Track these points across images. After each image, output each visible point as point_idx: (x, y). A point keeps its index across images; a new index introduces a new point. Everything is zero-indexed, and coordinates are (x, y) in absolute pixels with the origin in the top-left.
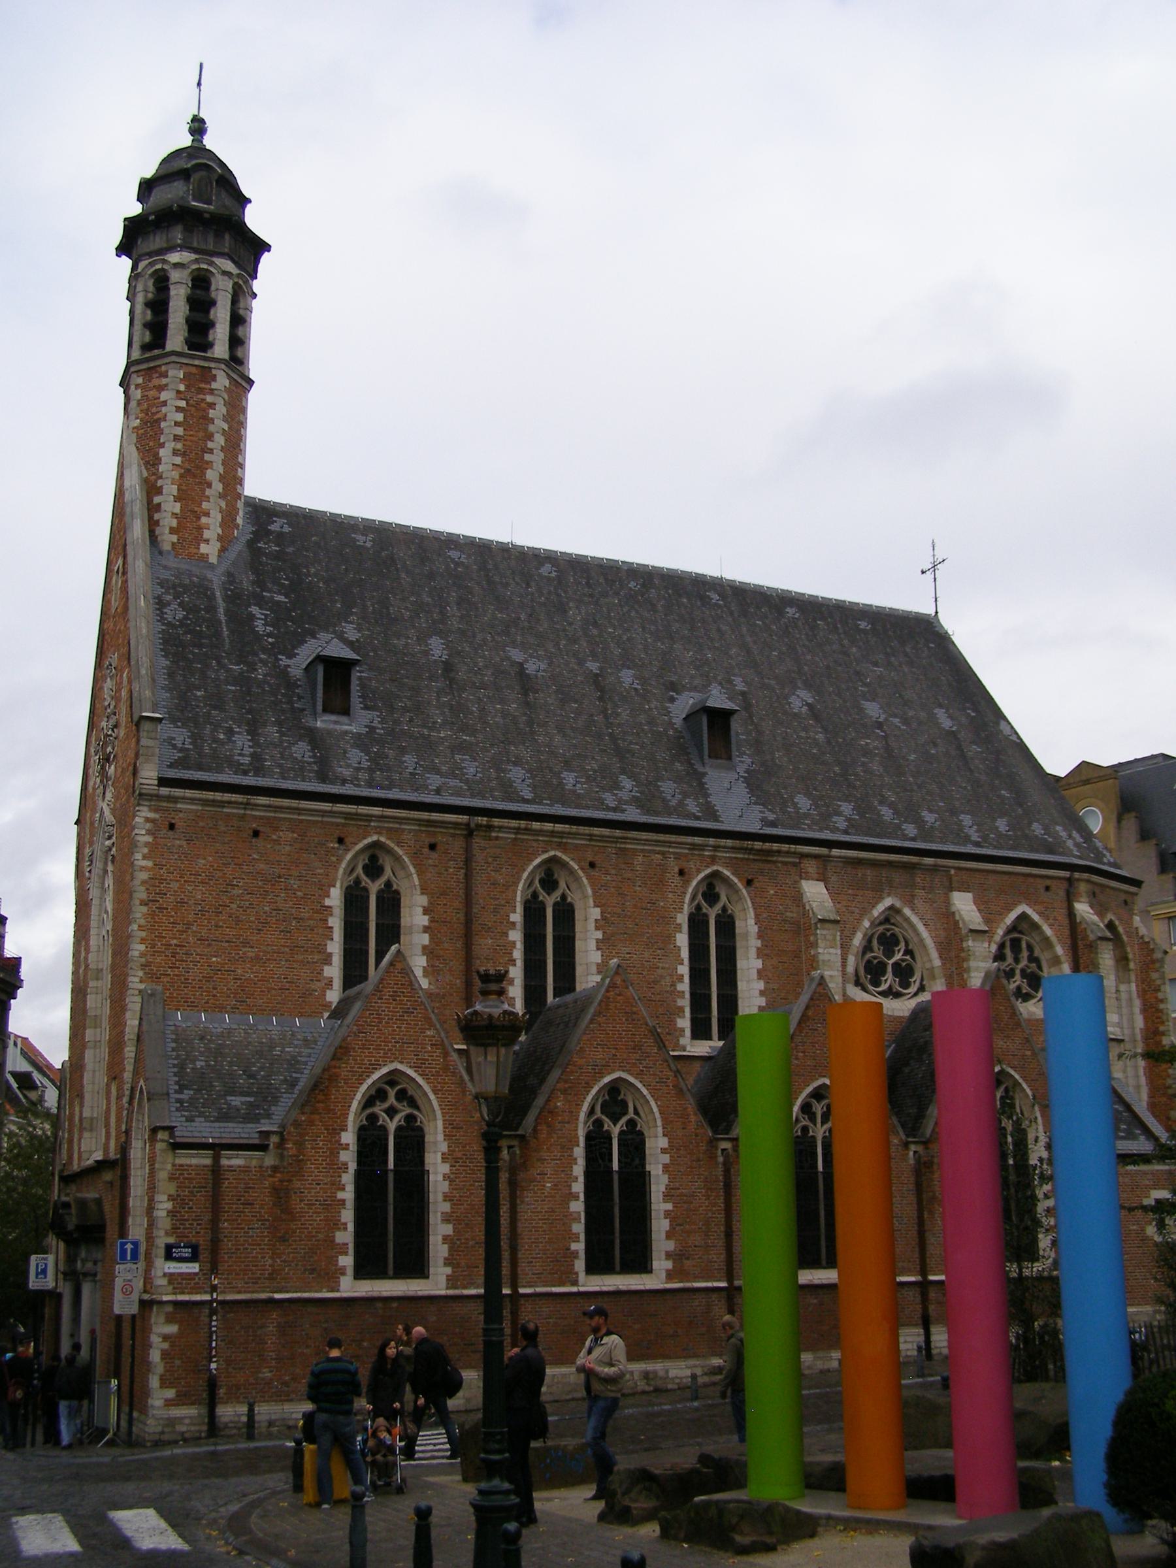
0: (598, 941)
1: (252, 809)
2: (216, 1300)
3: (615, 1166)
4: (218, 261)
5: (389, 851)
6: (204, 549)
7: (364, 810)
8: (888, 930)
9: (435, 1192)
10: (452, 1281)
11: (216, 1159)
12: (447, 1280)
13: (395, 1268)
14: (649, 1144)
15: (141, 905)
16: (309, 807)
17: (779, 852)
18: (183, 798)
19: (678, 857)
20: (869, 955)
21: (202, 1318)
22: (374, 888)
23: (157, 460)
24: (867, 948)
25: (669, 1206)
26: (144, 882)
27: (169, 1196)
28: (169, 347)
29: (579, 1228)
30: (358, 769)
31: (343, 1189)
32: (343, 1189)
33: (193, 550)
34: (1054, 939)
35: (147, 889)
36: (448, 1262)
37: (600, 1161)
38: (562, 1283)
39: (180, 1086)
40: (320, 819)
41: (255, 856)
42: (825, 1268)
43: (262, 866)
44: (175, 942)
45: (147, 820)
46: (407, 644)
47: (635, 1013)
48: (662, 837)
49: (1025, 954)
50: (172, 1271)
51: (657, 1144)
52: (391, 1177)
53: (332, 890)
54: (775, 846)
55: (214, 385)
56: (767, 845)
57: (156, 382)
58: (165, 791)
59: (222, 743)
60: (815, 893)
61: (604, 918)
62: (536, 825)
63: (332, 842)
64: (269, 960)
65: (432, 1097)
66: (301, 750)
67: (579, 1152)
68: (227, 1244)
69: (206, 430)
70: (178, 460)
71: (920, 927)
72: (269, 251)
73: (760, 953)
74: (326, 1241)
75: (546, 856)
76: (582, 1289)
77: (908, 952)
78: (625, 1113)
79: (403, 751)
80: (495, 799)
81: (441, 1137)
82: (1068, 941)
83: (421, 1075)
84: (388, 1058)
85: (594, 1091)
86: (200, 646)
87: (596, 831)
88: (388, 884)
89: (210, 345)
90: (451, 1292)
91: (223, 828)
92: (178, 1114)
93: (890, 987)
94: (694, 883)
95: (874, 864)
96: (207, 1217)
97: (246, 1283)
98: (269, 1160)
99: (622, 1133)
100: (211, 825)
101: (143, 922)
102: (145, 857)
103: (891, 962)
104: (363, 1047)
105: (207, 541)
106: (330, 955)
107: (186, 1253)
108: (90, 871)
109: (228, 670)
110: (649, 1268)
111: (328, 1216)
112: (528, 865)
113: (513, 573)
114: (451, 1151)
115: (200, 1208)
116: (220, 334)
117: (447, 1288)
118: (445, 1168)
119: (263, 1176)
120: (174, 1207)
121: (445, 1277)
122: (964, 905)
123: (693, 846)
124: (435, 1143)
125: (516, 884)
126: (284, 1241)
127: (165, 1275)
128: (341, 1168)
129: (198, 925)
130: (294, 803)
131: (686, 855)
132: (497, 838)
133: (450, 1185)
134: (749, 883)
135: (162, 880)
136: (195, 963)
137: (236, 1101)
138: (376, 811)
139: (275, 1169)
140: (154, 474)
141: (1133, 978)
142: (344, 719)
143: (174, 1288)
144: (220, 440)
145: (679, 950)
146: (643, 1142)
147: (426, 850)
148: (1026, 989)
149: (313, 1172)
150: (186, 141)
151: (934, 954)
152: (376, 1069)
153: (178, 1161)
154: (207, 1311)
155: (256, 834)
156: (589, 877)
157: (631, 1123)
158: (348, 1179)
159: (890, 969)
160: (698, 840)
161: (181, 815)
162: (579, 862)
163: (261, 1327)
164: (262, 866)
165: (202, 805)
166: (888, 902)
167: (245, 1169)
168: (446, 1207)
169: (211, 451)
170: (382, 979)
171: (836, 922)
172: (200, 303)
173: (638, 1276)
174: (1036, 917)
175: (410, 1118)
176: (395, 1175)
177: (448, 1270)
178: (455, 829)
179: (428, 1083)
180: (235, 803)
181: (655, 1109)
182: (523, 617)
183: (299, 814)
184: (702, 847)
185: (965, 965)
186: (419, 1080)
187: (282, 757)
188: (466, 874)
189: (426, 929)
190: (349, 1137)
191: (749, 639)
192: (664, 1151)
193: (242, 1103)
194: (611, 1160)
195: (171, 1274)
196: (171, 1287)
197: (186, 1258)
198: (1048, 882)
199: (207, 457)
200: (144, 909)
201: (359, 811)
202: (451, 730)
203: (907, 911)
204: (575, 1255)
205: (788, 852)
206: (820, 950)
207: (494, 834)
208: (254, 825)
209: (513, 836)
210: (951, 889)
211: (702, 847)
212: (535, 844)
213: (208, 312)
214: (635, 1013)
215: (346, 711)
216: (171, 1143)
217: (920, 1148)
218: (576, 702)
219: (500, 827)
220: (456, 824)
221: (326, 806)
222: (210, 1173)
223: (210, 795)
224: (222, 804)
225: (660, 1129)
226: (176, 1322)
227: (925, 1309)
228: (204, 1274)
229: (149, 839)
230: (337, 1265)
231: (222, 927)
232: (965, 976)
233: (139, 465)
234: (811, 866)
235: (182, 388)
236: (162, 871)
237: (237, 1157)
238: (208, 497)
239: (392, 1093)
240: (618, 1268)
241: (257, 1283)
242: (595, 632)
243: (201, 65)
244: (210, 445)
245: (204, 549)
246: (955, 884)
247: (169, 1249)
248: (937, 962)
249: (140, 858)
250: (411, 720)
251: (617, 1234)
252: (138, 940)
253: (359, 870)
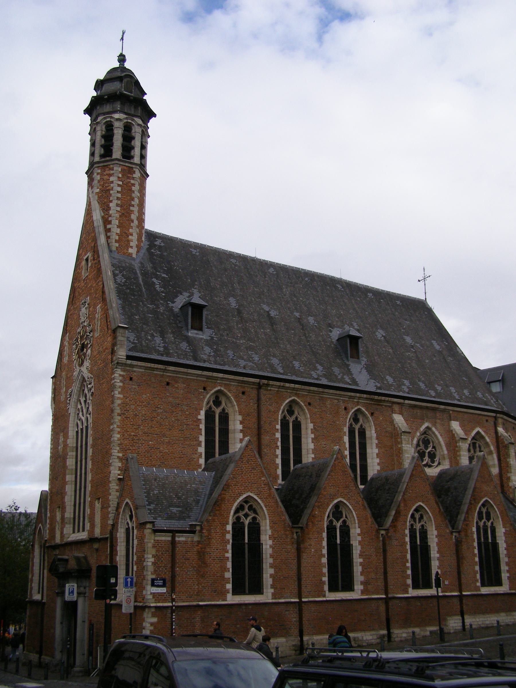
0: (312, 438)
1: (166, 372)
2: (174, 606)
3: (338, 541)
4: (136, 119)
5: (225, 394)
6: (130, 250)
7: (215, 374)
8: (426, 437)
9: (266, 554)
10: (274, 596)
11: (173, 537)
12: (272, 595)
13: (249, 590)
14: (352, 531)
15: (118, 415)
16: (191, 372)
17: (384, 401)
18: (137, 366)
19: (344, 401)
20: (419, 448)
21: (168, 615)
22: (218, 411)
23: (109, 208)
24: (418, 445)
25: (361, 560)
26: (119, 405)
27: (153, 555)
28: (114, 156)
29: (325, 570)
30: (210, 356)
31: (228, 552)
32: (228, 552)
33: (126, 251)
34: (490, 443)
35: (121, 408)
36: (272, 586)
37: (332, 539)
38: (319, 596)
39: (149, 502)
40: (195, 378)
41: (168, 394)
42: (422, 589)
43: (171, 399)
44: (133, 434)
45: (120, 375)
46: (220, 300)
47: (346, 471)
48: (338, 392)
49: (478, 449)
50: (154, 591)
51: (355, 531)
52: (246, 546)
53: (201, 411)
54: (383, 398)
55: (134, 176)
56: (380, 398)
57: (107, 172)
58: (129, 362)
59: (150, 341)
60: (399, 419)
61: (315, 428)
62: (287, 385)
63: (201, 389)
64: (174, 443)
65: (264, 509)
66: (184, 345)
67: (325, 535)
68: (178, 579)
69: (131, 196)
70: (119, 209)
72: (155, 117)
73: (377, 446)
74: (221, 577)
75: (290, 399)
76: (328, 599)
77: (434, 447)
78: (342, 517)
79: (226, 348)
80: (268, 372)
81: (268, 528)
82: (495, 444)
83: (260, 498)
84: (246, 491)
85: (330, 507)
86: (134, 295)
87: (312, 388)
88: (224, 410)
89: (132, 157)
90: (274, 601)
91: (154, 381)
92: (149, 516)
93: (427, 463)
94: (351, 413)
95: (421, 407)
96: (169, 565)
97: (187, 597)
98: (196, 538)
99: (341, 526)
100: (148, 379)
101: (118, 424)
102: (119, 393)
103: (427, 451)
104: (235, 485)
105: (132, 247)
106: (201, 442)
107: (161, 583)
108: (70, 400)
109: (148, 307)
110: (353, 589)
111: (221, 565)
112: (283, 403)
113: (258, 270)
114: (273, 534)
115: (166, 561)
116: (137, 152)
117: (272, 599)
118: (270, 542)
119: (194, 546)
120: (155, 561)
121: (271, 594)
122: (455, 426)
123: (350, 397)
124: (266, 530)
125: (278, 411)
126: (203, 577)
127: (151, 593)
128: (227, 542)
129: (143, 426)
130: (185, 370)
131: (347, 401)
132: (270, 390)
133: (273, 550)
134: (372, 414)
135: (127, 404)
136: (142, 444)
137: (174, 510)
138: (221, 375)
139: (199, 542)
140: (107, 214)
142: (200, 332)
143: (155, 600)
144: (137, 201)
145: (345, 444)
146: (349, 531)
147: (241, 394)
149: (215, 544)
150: (117, 65)
151: (444, 448)
152: (241, 495)
153: (157, 538)
154: (170, 611)
155: (168, 384)
156: (308, 409)
157: (344, 522)
158: (229, 547)
159: (427, 454)
160: (352, 394)
161: (135, 374)
162: (304, 402)
163: (193, 619)
164: (171, 399)
165: (145, 369)
166: (426, 425)
167: (185, 542)
168: (271, 560)
169: (133, 206)
170: (243, 453)
171: (409, 433)
172: (128, 138)
173: (348, 593)
174: (483, 433)
175: (254, 519)
176: (248, 545)
177: (272, 590)
178: (253, 385)
179: (263, 502)
180: (160, 369)
181: (355, 515)
182: (265, 291)
183: (187, 375)
184: (354, 397)
185: (458, 453)
186: (259, 500)
187: (177, 349)
188: (258, 406)
189: (241, 431)
190: (229, 528)
191: (356, 306)
192: (359, 535)
193: (177, 511)
194: (336, 539)
195: (154, 593)
196: (154, 599)
197: (160, 585)
198: (487, 418)
199: (131, 208)
200: (119, 418)
201: (214, 375)
202: (245, 339)
203: (434, 429)
204: (324, 583)
205: (388, 401)
206: (403, 445)
207: (269, 388)
208: (167, 380)
209: (277, 389)
210: (451, 420)
211: (354, 397)
212: (286, 393)
213: (130, 142)
214: (346, 471)
215: (201, 329)
216: (153, 530)
217: (457, 534)
218: (293, 330)
219: (272, 385)
220: (254, 383)
221: (199, 372)
222: (170, 544)
223: (149, 365)
224: (153, 369)
225: (357, 525)
226: (156, 617)
227: (462, 607)
228: (168, 593)
229: (121, 384)
230: (225, 588)
231: (154, 427)
232: (458, 458)
233: (100, 210)
234: (396, 408)
235: (120, 176)
236: (127, 400)
237: (182, 536)
238: (132, 227)
239: (246, 507)
240: (340, 589)
241: (191, 597)
242: (295, 299)
244: (133, 203)
245: (130, 250)
246: (452, 418)
247: (153, 580)
248: (446, 452)
249: (117, 393)
250: (228, 335)
251: (340, 573)
252: (117, 432)
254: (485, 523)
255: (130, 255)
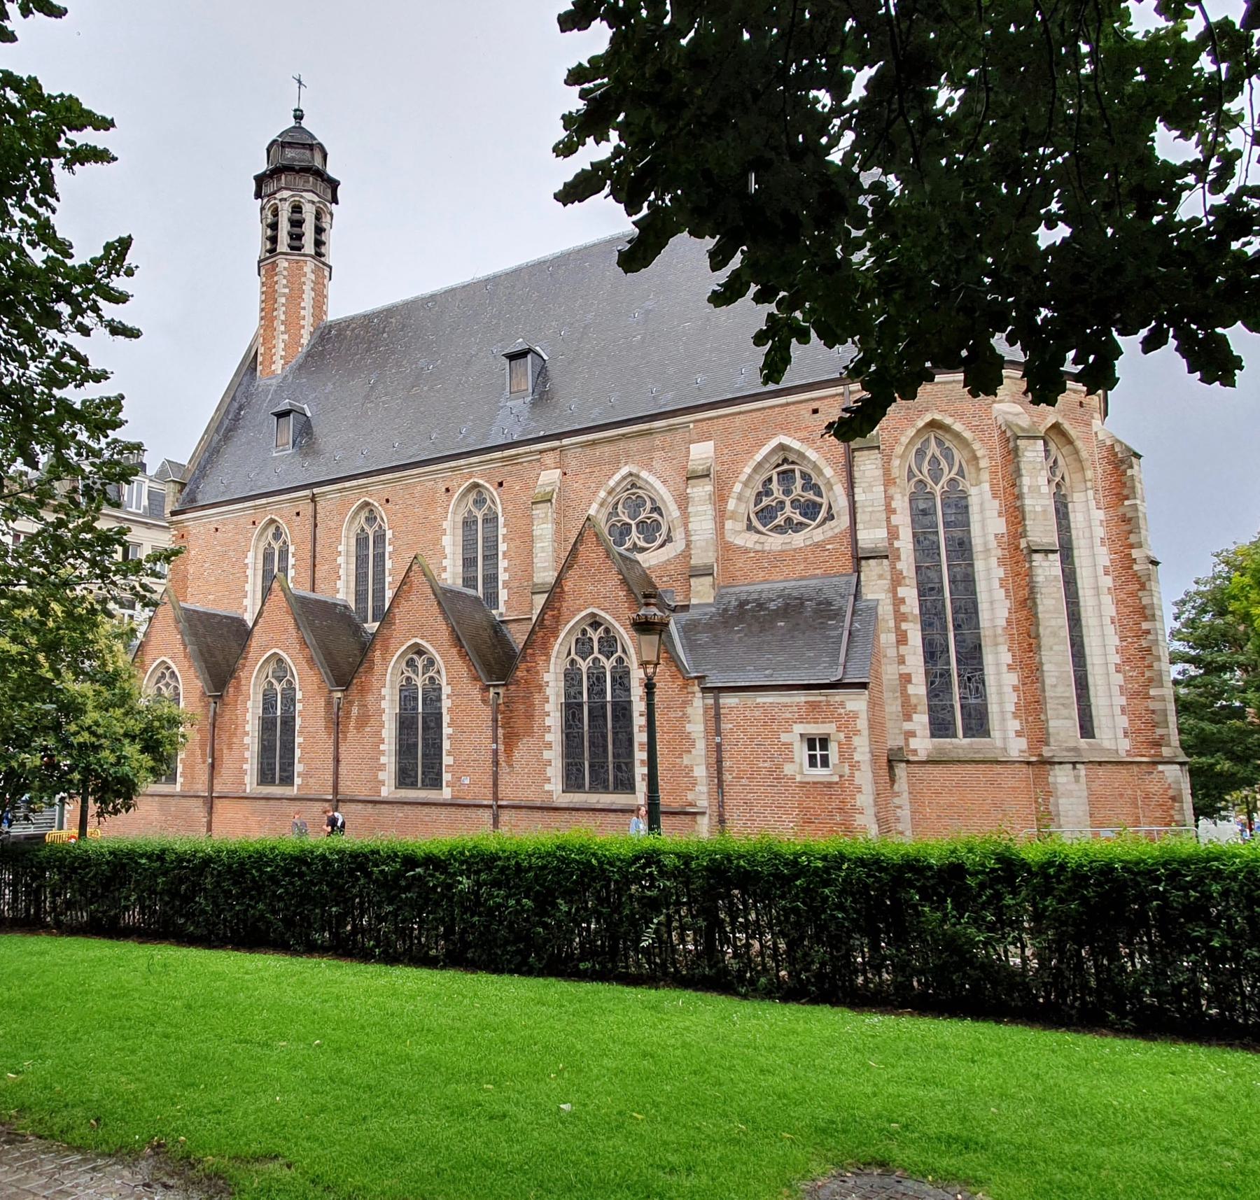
4: (304, 194)
49: (799, 482)
71: (658, 485)
141: (985, 476)
148: (798, 517)
174: (796, 445)
254: (596, 660)
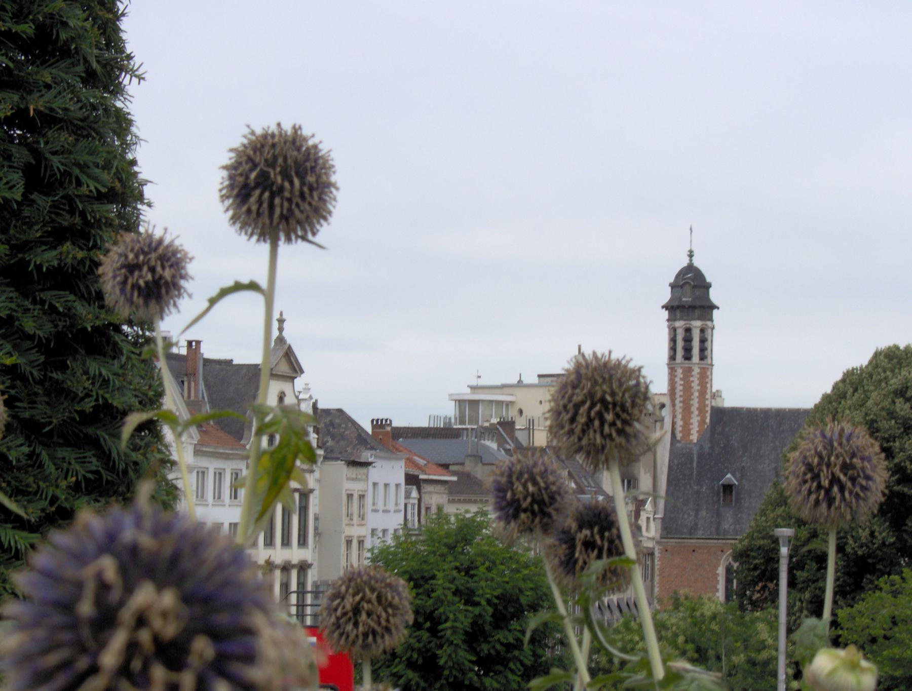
116: (696, 351)
150: (685, 262)
243: (691, 229)
245: (691, 437)
253: (731, 559)
255: (692, 440)
